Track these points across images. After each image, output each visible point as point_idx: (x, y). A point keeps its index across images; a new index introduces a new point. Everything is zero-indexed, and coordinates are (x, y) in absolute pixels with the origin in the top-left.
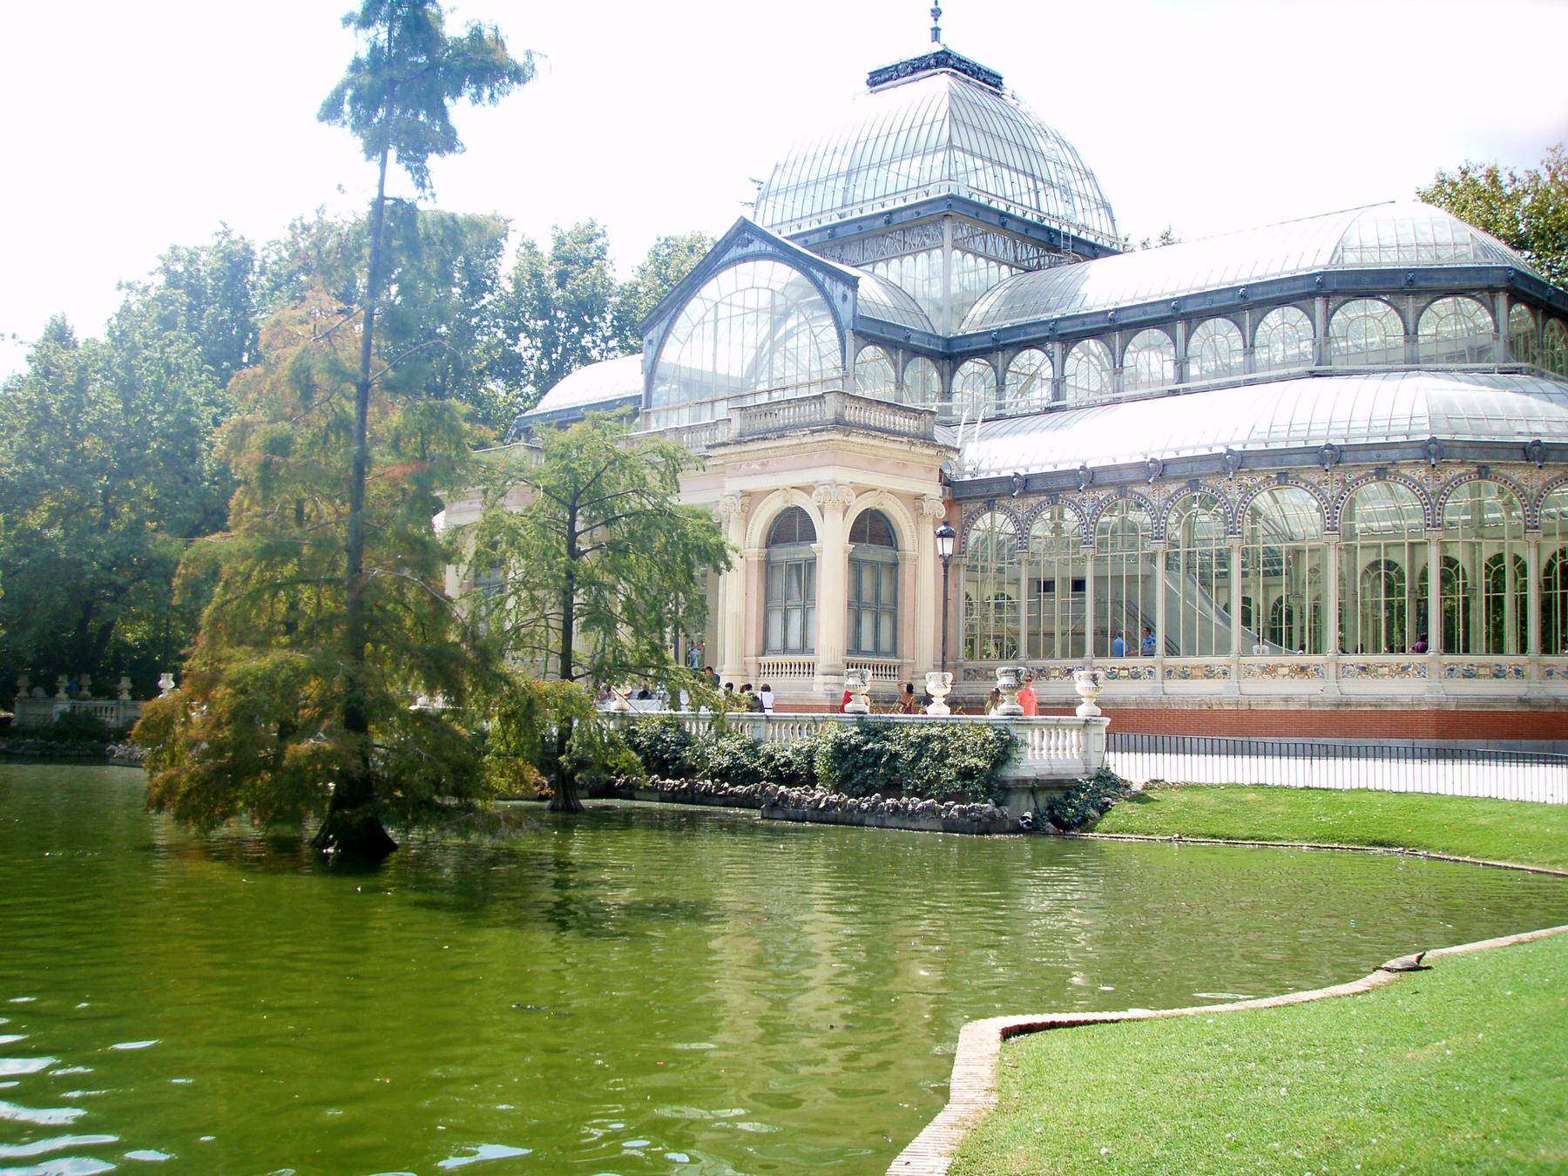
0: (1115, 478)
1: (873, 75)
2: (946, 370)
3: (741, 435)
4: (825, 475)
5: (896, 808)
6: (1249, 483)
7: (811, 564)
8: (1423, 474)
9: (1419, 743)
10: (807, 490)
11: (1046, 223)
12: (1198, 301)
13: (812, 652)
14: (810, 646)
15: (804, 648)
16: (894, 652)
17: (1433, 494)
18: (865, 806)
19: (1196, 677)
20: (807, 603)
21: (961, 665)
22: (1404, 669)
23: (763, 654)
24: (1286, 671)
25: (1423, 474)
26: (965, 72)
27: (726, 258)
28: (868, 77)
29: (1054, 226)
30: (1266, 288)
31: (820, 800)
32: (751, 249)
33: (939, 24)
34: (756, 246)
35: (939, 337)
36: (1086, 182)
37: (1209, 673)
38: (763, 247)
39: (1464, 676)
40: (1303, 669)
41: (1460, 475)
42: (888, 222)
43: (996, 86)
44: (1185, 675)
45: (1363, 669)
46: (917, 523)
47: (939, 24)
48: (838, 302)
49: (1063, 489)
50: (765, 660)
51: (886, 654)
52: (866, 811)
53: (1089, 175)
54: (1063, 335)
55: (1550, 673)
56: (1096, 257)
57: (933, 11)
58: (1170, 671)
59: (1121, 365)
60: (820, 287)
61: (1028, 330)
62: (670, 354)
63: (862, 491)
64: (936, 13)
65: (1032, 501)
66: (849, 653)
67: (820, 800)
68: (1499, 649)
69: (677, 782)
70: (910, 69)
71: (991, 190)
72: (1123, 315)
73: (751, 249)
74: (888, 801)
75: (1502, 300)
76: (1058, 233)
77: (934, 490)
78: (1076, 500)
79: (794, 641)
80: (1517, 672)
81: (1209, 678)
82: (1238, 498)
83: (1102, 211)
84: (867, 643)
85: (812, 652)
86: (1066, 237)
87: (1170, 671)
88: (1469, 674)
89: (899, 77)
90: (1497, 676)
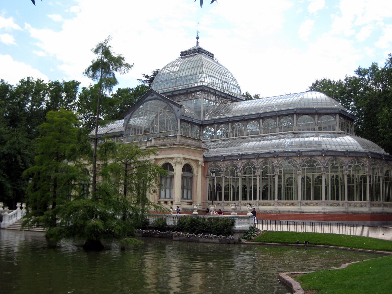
0: (247, 157)
1: (182, 53)
2: (202, 128)
3: (154, 145)
4: (176, 155)
5: (207, 237)
6: (280, 159)
7: (172, 177)
8: (321, 158)
9: (320, 221)
10: (172, 158)
11: (225, 92)
13: (172, 198)
14: (172, 197)
15: (170, 197)
16: (191, 198)
17: (323, 163)
18: (199, 236)
19: (266, 206)
20: (171, 187)
21: (207, 202)
22: (316, 204)
23: (159, 199)
24: (288, 204)
25: (321, 158)
26: (205, 54)
27: (147, 99)
28: (181, 53)
29: (227, 93)
30: (282, 112)
31: (188, 235)
33: (199, 41)
34: (155, 96)
35: (200, 121)
36: (234, 82)
37: (270, 205)
38: (157, 97)
39: (331, 206)
40: (292, 204)
41: (329, 159)
42: (187, 91)
43: (212, 57)
44: (264, 205)
45: (307, 204)
46: (197, 167)
47: (199, 41)
49: (234, 160)
50: (160, 200)
51: (190, 199)
52: (200, 238)
53: (235, 80)
54: (231, 121)
55: (350, 205)
56: (236, 101)
57: (197, 37)
58: (260, 204)
59: (246, 129)
61: (223, 119)
62: (131, 122)
63: (185, 159)
64: (198, 38)
65: (226, 162)
66: (181, 199)
67: (188, 235)
68: (337, 199)
69: (146, 231)
70: (191, 52)
71: (208, 83)
72: (247, 116)
74: (205, 235)
75: (338, 117)
76: (228, 95)
77: (201, 159)
78: (237, 162)
79: (167, 196)
80: (343, 205)
81: (269, 206)
82: (277, 163)
83: (238, 89)
84: (185, 197)
85: (172, 198)
86: (230, 96)
87: (260, 204)
88: (331, 205)
90: (338, 206)
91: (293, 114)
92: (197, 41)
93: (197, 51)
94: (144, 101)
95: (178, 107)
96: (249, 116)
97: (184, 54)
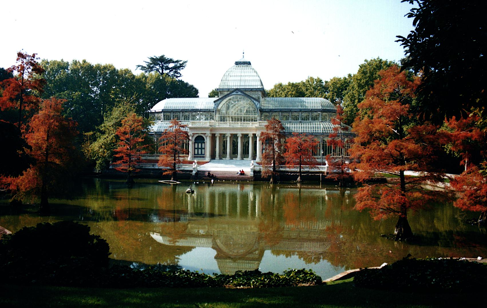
27: (233, 94)
32: (238, 93)
38: (241, 94)
47: (244, 55)
48: (256, 104)
60: (253, 102)
64: (243, 53)
73: (238, 93)
97: (237, 63)
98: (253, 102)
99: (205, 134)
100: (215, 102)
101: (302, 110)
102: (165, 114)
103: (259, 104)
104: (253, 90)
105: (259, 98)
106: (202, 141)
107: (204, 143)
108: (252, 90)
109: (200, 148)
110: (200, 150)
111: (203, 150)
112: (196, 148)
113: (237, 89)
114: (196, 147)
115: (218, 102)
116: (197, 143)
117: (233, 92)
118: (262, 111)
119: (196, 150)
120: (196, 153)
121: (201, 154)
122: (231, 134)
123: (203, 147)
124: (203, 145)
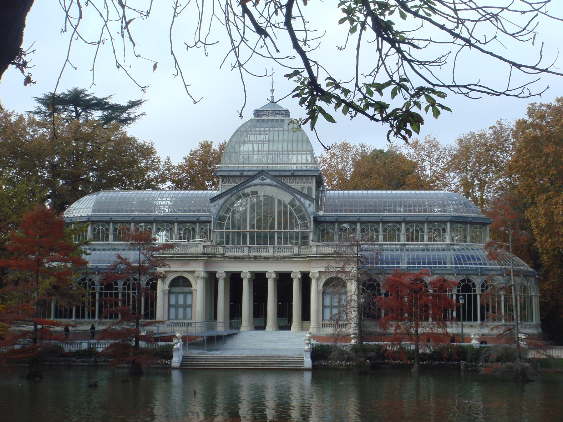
12: (411, 218)
24: (468, 326)
27: (253, 182)
32: (265, 181)
33: (274, 95)
38: (272, 182)
40: (472, 326)
47: (274, 95)
64: (272, 91)
73: (265, 181)
89: (268, 116)
91: (447, 222)
92: (271, 95)
93: (284, 113)
94: (248, 185)
95: (310, 200)
96: (388, 218)
98: (299, 200)
99: (194, 272)
100: (213, 200)
101: (408, 219)
102: (95, 226)
103: (312, 206)
104: (296, 174)
105: (310, 189)
106: (187, 289)
107: (191, 293)
108: (294, 175)
109: (181, 306)
110: (181, 310)
111: (189, 310)
112: (173, 306)
113: (261, 173)
114: (173, 302)
115: (221, 201)
116: (174, 293)
117: (253, 178)
118: (317, 221)
119: (173, 310)
120: (172, 316)
121: (185, 318)
122: (252, 273)
123: (189, 302)
124: (189, 297)
